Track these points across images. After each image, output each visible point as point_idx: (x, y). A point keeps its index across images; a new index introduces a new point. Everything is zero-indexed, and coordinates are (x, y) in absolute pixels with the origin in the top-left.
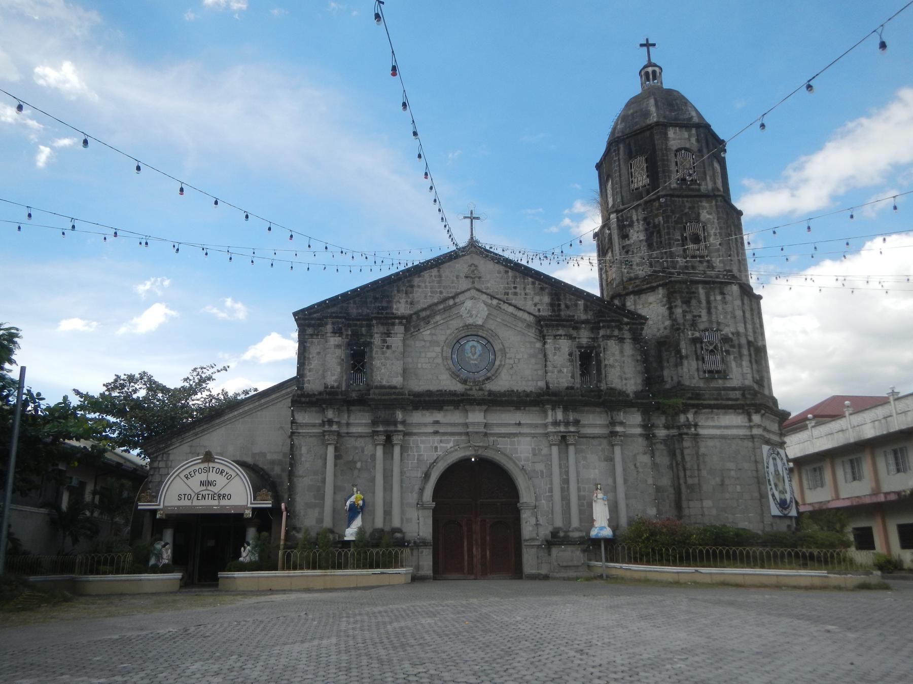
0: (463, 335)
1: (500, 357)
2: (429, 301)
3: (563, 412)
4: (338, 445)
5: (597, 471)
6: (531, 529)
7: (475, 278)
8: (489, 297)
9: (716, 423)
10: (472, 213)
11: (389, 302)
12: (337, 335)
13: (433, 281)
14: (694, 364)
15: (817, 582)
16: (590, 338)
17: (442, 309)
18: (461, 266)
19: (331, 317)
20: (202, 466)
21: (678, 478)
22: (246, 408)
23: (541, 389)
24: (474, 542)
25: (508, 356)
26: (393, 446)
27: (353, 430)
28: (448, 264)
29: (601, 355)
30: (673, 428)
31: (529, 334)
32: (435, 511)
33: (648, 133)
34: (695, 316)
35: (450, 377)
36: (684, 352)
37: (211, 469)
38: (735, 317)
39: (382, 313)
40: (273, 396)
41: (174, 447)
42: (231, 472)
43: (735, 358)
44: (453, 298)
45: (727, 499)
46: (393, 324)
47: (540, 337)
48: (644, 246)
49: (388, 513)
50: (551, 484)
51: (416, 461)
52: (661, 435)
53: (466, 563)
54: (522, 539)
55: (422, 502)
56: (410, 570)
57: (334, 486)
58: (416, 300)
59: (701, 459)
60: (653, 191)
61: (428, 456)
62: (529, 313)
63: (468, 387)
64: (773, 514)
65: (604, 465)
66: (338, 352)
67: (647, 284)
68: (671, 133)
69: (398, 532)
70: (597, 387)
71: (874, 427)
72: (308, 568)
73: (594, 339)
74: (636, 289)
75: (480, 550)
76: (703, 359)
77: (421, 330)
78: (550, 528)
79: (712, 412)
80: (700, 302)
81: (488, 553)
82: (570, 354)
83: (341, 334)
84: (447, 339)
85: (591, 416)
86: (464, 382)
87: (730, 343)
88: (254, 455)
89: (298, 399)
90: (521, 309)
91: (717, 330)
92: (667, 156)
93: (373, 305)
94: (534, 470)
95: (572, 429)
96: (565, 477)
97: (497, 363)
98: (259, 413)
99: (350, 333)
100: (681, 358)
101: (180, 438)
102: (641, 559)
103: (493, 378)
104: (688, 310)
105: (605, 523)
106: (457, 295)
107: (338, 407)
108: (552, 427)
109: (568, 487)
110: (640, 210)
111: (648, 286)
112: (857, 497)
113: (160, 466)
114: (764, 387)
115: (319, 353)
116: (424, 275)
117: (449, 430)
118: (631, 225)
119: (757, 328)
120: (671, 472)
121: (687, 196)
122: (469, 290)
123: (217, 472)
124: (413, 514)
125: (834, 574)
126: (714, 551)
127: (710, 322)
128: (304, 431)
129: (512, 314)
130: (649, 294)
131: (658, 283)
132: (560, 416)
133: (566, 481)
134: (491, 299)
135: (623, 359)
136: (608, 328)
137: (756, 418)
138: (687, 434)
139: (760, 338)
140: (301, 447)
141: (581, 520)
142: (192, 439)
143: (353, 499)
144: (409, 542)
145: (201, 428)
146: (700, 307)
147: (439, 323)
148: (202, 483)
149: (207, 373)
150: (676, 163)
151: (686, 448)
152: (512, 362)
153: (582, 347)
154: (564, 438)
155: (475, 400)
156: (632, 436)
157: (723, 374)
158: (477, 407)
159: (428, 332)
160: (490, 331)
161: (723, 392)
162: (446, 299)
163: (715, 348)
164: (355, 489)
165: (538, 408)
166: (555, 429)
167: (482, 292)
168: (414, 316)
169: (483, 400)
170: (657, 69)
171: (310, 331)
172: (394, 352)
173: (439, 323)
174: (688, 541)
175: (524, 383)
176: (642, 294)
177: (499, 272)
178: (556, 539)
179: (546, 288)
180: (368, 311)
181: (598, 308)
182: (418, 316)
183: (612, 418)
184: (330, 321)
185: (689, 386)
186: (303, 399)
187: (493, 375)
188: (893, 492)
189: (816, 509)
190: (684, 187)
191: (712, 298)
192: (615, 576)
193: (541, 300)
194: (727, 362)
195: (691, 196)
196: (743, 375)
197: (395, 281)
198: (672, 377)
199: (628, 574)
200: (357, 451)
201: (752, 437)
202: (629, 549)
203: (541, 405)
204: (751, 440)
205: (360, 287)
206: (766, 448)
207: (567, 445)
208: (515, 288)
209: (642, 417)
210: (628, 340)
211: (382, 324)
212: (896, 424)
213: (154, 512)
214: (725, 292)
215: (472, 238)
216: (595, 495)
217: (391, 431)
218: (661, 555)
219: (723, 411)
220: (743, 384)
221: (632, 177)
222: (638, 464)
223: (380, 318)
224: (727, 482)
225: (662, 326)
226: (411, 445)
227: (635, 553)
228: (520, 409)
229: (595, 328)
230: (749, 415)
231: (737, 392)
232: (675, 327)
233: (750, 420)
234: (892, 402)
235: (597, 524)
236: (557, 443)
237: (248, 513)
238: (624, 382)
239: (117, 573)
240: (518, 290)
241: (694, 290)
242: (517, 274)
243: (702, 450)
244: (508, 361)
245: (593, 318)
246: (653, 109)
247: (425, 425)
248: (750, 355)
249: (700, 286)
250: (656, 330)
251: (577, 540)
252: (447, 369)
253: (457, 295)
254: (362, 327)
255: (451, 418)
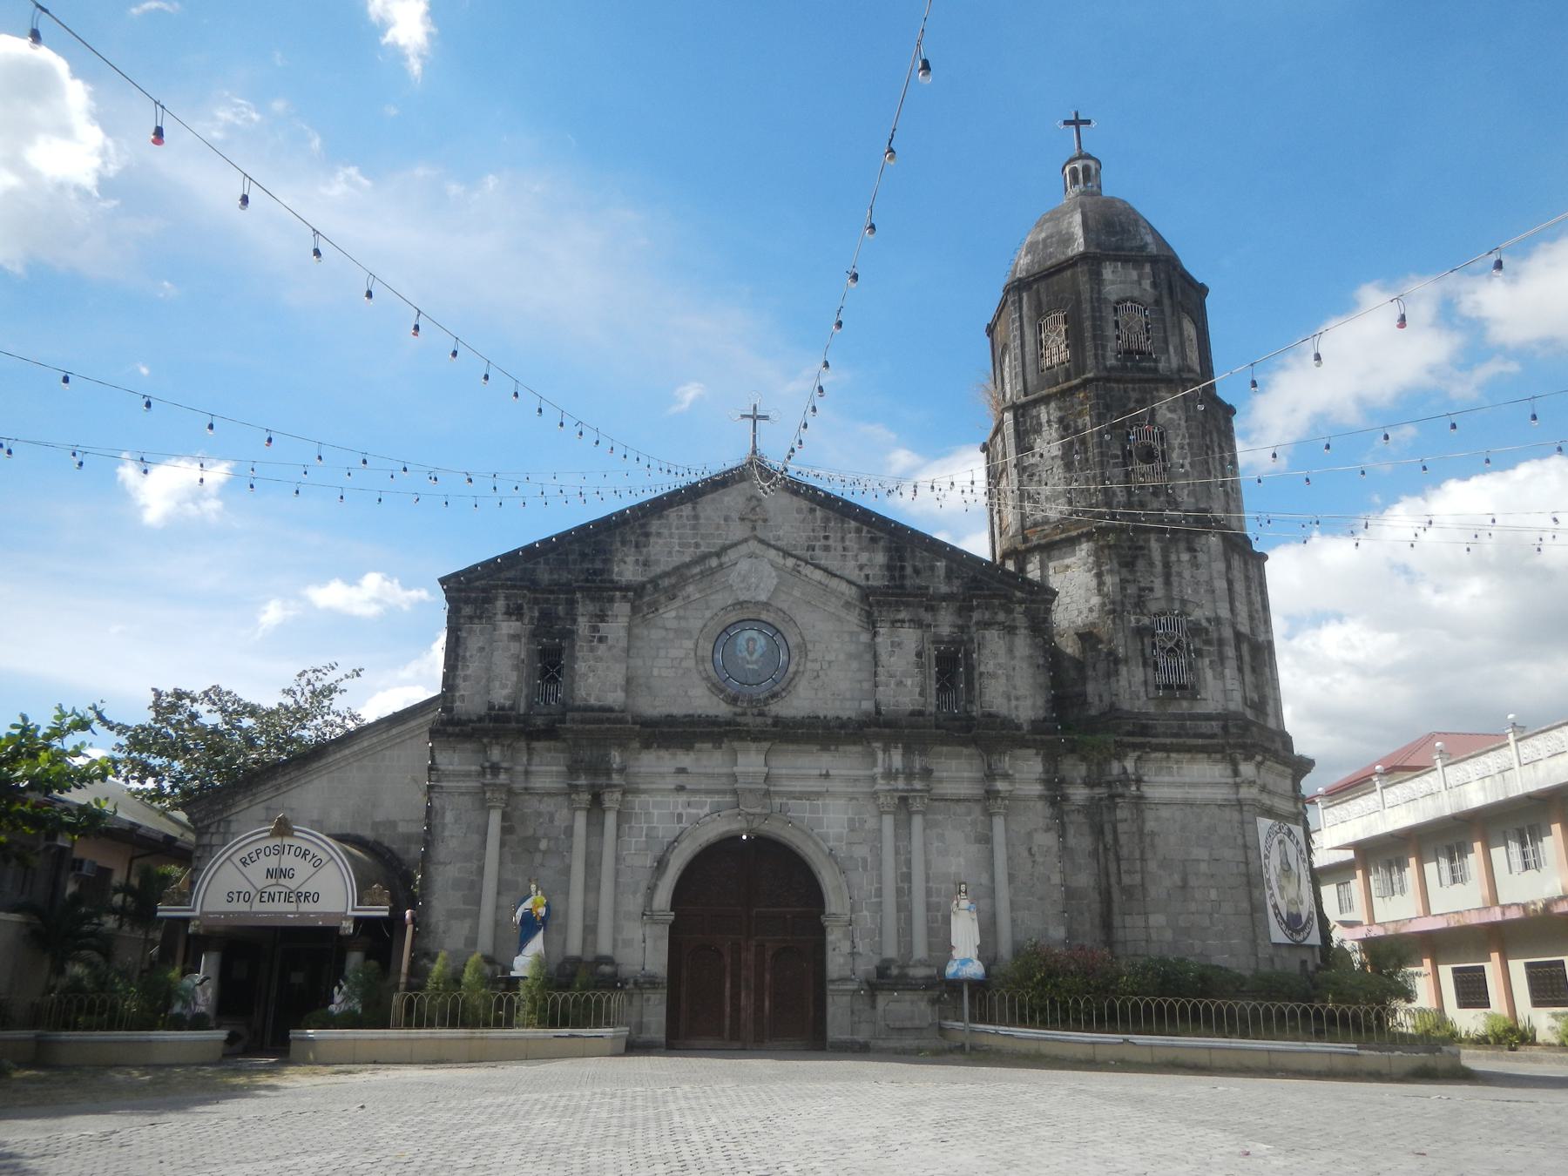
0: (734, 619)
1: (797, 658)
2: (676, 560)
3: (903, 755)
4: (509, 809)
5: (962, 860)
6: (842, 960)
7: (756, 521)
8: (781, 554)
9: (1177, 779)
10: (755, 408)
11: (605, 561)
12: (514, 618)
13: (684, 526)
14: (1139, 674)
15: (1340, 1063)
16: (954, 626)
17: (696, 575)
18: (732, 499)
19: (503, 586)
20: (272, 843)
21: (1108, 875)
22: (366, 744)
23: (867, 714)
24: (743, 984)
25: (810, 657)
26: (604, 811)
27: (538, 783)
28: (710, 496)
29: (975, 656)
30: (1099, 785)
31: (848, 618)
32: (673, 928)
33: (1068, 273)
34: (1142, 589)
35: (707, 693)
37: (287, 848)
38: (1213, 592)
39: (594, 581)
40: (413, 724)
41: (238, 810)
42: (321, 855)
43: (1211, 662)
44: (718, 555)
45: (1193, 913)
46: (611, 600)
47: (868, 623)
49: (590, 930)
50: (880, 876)
51: (644, 839)
52: (1078, 797)
53: (727, 1022)
54: (828, 979)
55: (651, 911)
56: (624, 1031)
57: (499, 879)
58: (653, 558)
59: (1148, 840)
60: (1077, 375)
61: (665, 829)
62: (850, 582)
63: (738, 710)
64: (1273, 941)
65: (974, 849)
66: (515, 647)
67: (1062, 532)
68: (1108, 273)
69: (606, 964)
70: (966, 711)
71: (1484, 789)
72: (442, 1025)
73: (962, 629)
74: (1043, 541)
75: (752, 997)
76: (1156, 663)
77: (661, 611)
78: (876, 961)
79: (1168, 757)
80: (1151, 564)
81: (767, 1003)
82: (919, 655)
83: (520, 616)
84: (705, 626)
85: (954, 763)
86: (734, 700)
87: (1204, 637)
88: (375, 825)
89: (441, 728)
90: (835, 576)
91: (1181, 614)
92: (1101, 312)
93: (578, 567)
94: (851, 857)
95: (918, 785)
96: (905, 870)
97: (792, 668)
98: (387, 753)
99: (537, 614)
100: (1117, 661)
101: (250, 793)
102: (1032, 1018)
103: (784, 694)
104: (1130, 577)
105: (972, 953)
106: (724, 549)
107: (509, 742)
108: (880, 781)
109: (910, 888)
110: (1053, 405)
111: (1063, 536)
112: (1457, 912)
113: (213, 843)
114: (1266, 715)
115: (482, 649)
116: (668, 516)
117: (704, 784)
118: (1038, 430)
119: (1257, 611)
120: (1096, 865)
121: (1133, 381)
122: (746, 540)
123: (297, 853)
124: (634, 931)
125: (1370, 1049)
126: (1159, 1006)
127: (1170, 599)
128: (451, 784)
129: (820, 583)
130: (1064, 550)
131: (1080, 531)
132: (897, 759)
133: (907, 877)
134: (784, 557)
135: (1012, 663)
136: (987, 609)
137: (1247, 769)
138: (1122, 796)
139: (1262, 628)
140: (444, 813)
141: (930, 947)
142: (271, 795)
143: (528, 904)
144: (625, 982)
145: (287, 777)
146: (1152, 574)
147: (692, 598)
148: (270, 873)
149: (329, 680)
150: (1117, 323)
151: (1121, 821)
152: (817, 666)
153: (942, 642)
154: (904, 800)
155: (748, 732)
156: (1026, 799)
157: (1190, 691)
158: (753, 746)
159: (673, 614)
160: (782, 614)
161: (1188, 723)
162: (704, 557)
163: (1177, 645)
164: (533, 887)
165: (859, 748)
166: (888, 784)
167: (769, 545)
168: (649, 586)
169: (762, 732)
170: (1092, 164)
171: (467, 610)
172: (610, 648)
173: (692, 598)
174: (1112, 987)
175: (838, 703)
176: (1053, 550)
177: (799, 511)
178: (884, 980)
179: (881, 538)
180: (570, 576)
181: (971, 574)
182: (656, 587)
183: (989, 766)
184: (501, 593)
185: (1128, 712)
186: (450, 729)
187: (783, 690)
188: (1517, 905)
189: (1390, 933)
190: (1129, 364)
191: (1173, 558)
192: (986, 1048)
193: (870, 560)
194: (1198, 669)
195: (1140, 380)
196: (1225, 691)
197: (617, 525)
198: (1100, 696)
199: (1009, 1045)
200: (541, 820)
201: (1240, 804)
202: (1012, 999)
203: (865, 743)
204: (1238, 808)
205: (557, 536)
206: (1264, 824)
207: (910, 814)
208: (826, 538)
209: (1044, 765)
210: (1023, 631)
211: (593, 599)
212: (1520, 784)
213: (187, 920)
214: (1198, 547)
215: (754, 452)
216: (955, 902)
217: (601, 786)
218: (1065, 1011)
219: (1189, 756)
220: (1225, 710)
221: (1041, 348)
222: (1035, 849)
223: (589, 589)
224: (1193, 882)
225: (1084, 608)
226: (637, 810)
227: (1022, 1007)
228: (829, 750)
229: (964, 610)
230: (1235, 765)
231: (1213, 723)
232: (1106, 608)
233: (1236, 773)
234: (1513, 744)
235: (957, 954)
236: (892, 809)
237: (348, 927)
238: (1014, 703)
239: (110, 1028)
240: (831, 542)
241: (1141, 543)
242: (831, 514)
243: (1150, 825)
244: (809, 665)
245: (961, 591)
246: (1078, 231)
247: (662, 775)
248: (1240, 658)
249: (1153, 537)
250: (1076, 613)
251: (920, 982)
252: (704, 679)
253: (724, 549)
254: (557, 604)
255: (707, 762)
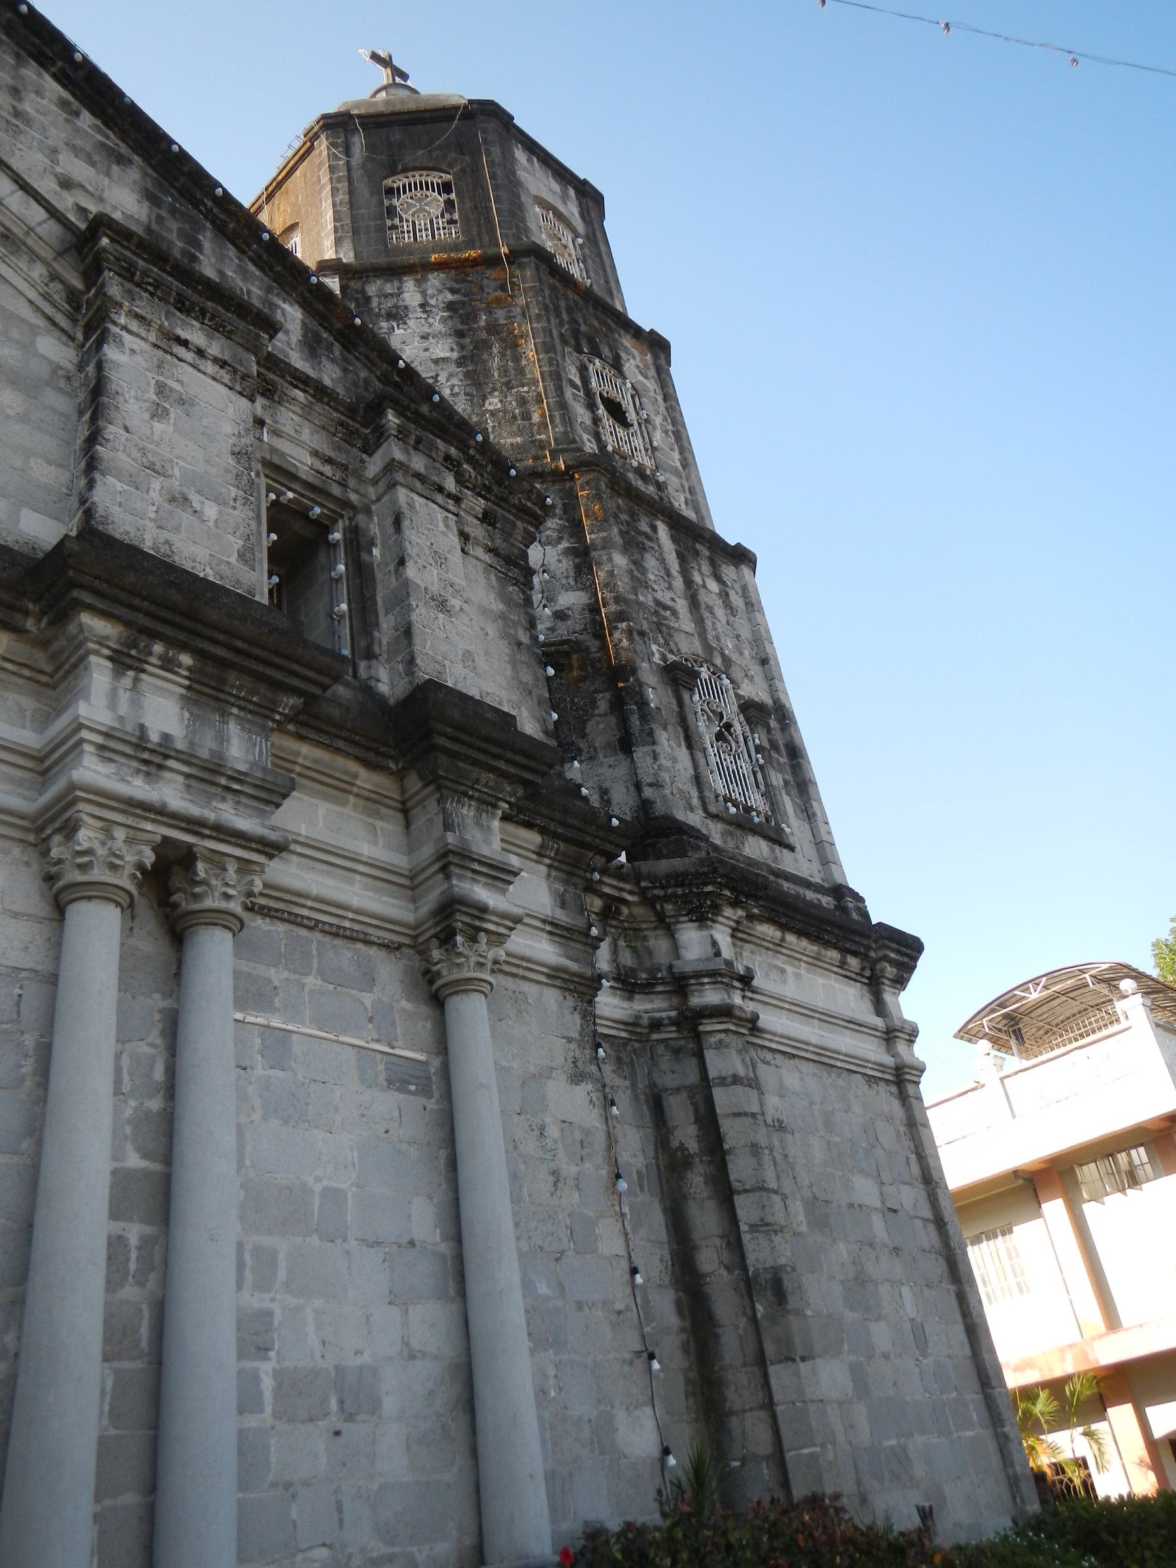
14: (683, 753)
34: (658, 603)
36: (651, 694)
43: (786, 783)
48: (451, 376)
65: (387, 1103)
96: (134, 1161)
191: (697, 578)
198: (604, 792)
204: (894, 1089)
210: (480, 552)
222: (553, 1131)
241: (644, 527)
